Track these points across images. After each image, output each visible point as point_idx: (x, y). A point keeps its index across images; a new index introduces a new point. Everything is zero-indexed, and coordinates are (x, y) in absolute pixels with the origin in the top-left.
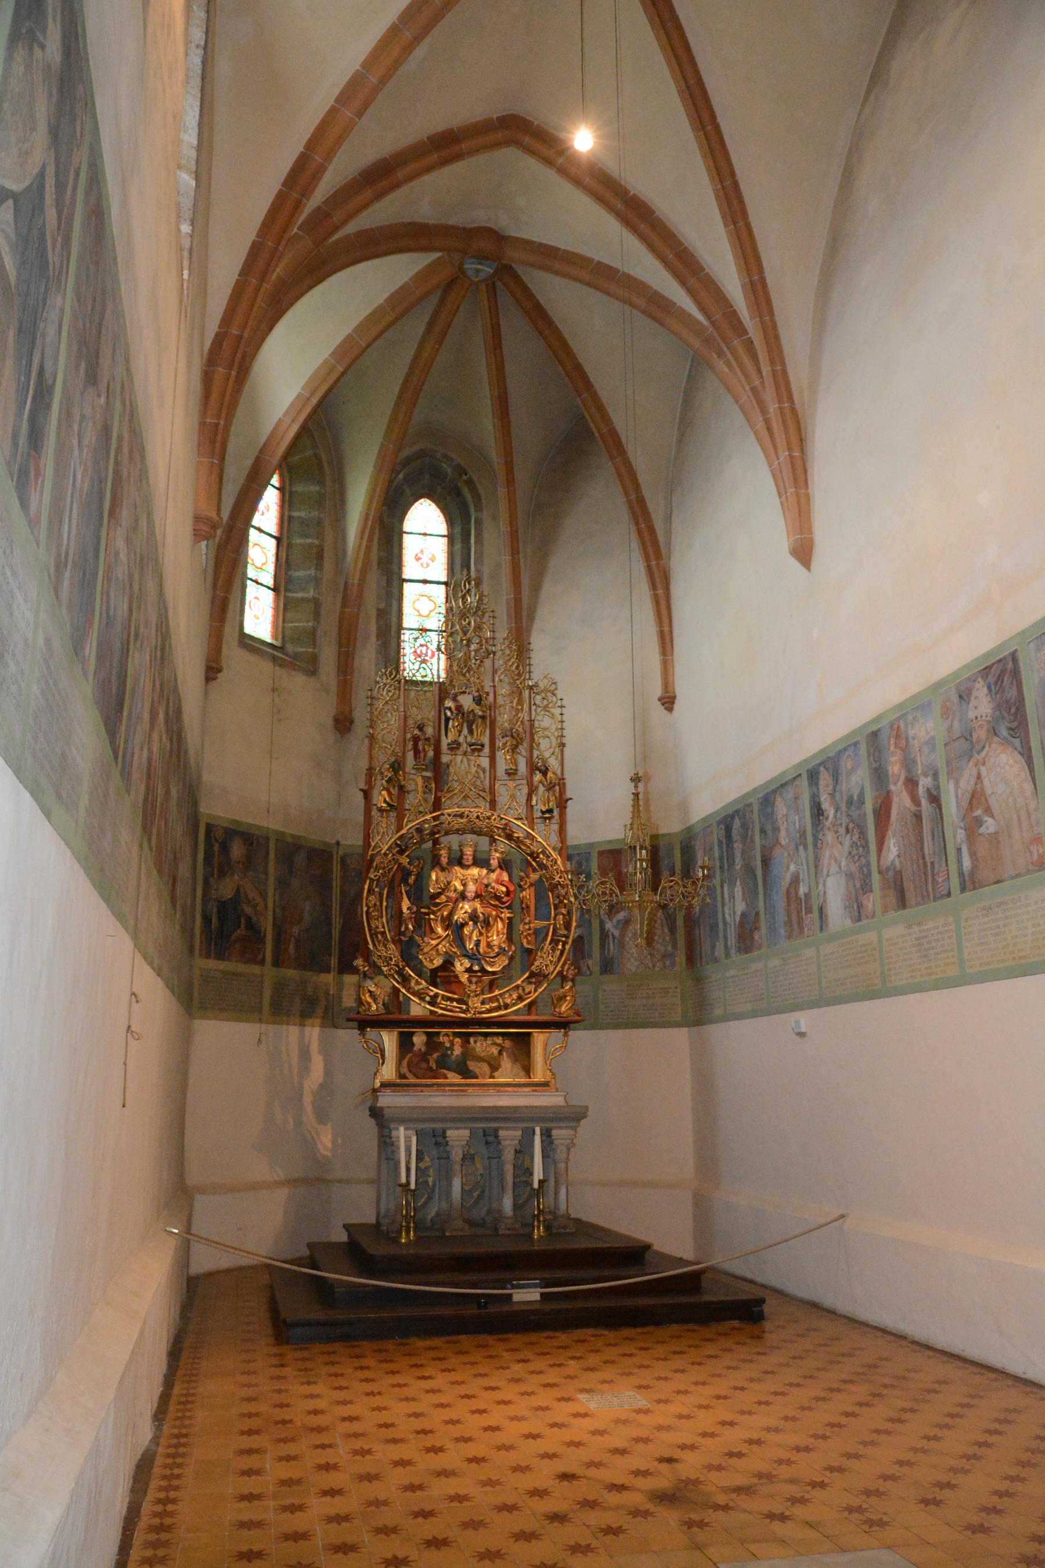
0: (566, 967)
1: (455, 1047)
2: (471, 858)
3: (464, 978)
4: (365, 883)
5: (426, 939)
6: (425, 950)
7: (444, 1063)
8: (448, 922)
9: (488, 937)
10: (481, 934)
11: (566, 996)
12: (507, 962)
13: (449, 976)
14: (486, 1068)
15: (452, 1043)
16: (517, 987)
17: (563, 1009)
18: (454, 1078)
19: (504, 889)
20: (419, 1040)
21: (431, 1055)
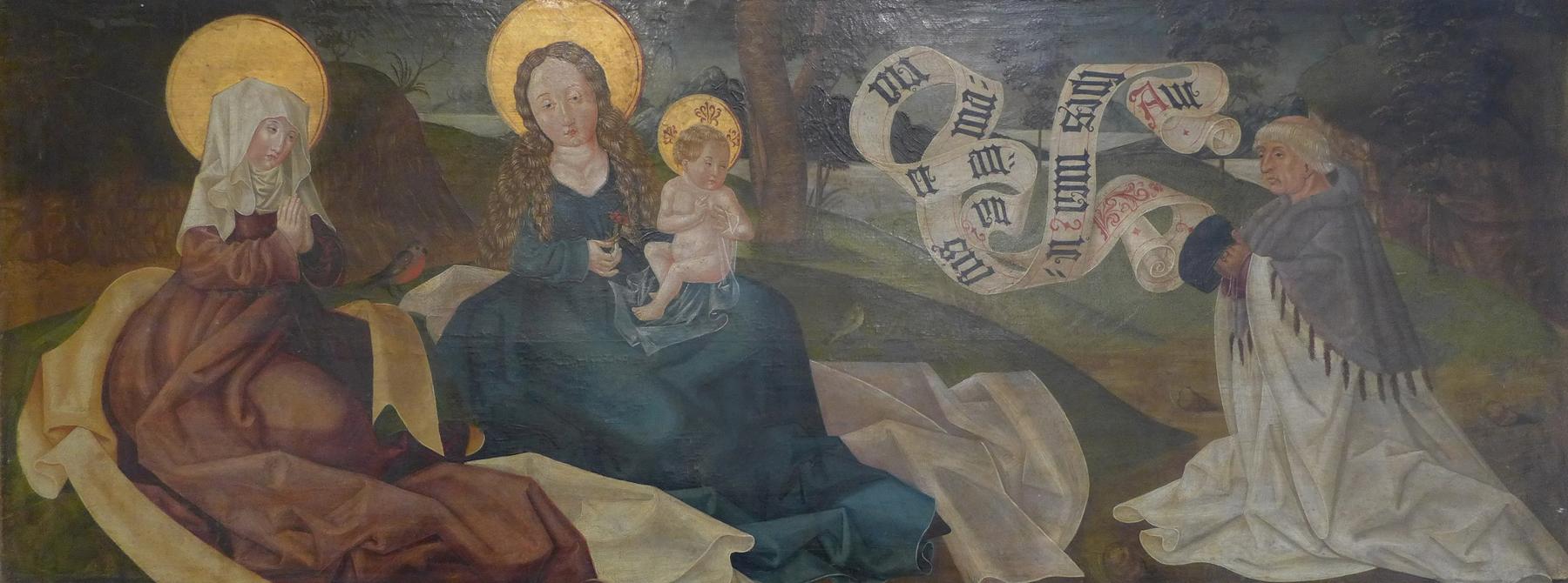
1: (677, 203)
21: (385, 285)
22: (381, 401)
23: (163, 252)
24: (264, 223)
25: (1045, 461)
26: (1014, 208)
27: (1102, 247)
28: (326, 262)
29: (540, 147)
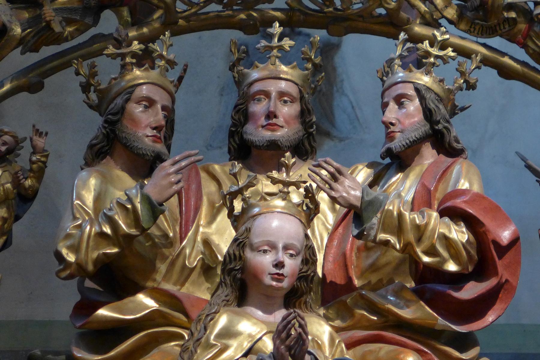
2: (287, 111)
19: (459, 234)
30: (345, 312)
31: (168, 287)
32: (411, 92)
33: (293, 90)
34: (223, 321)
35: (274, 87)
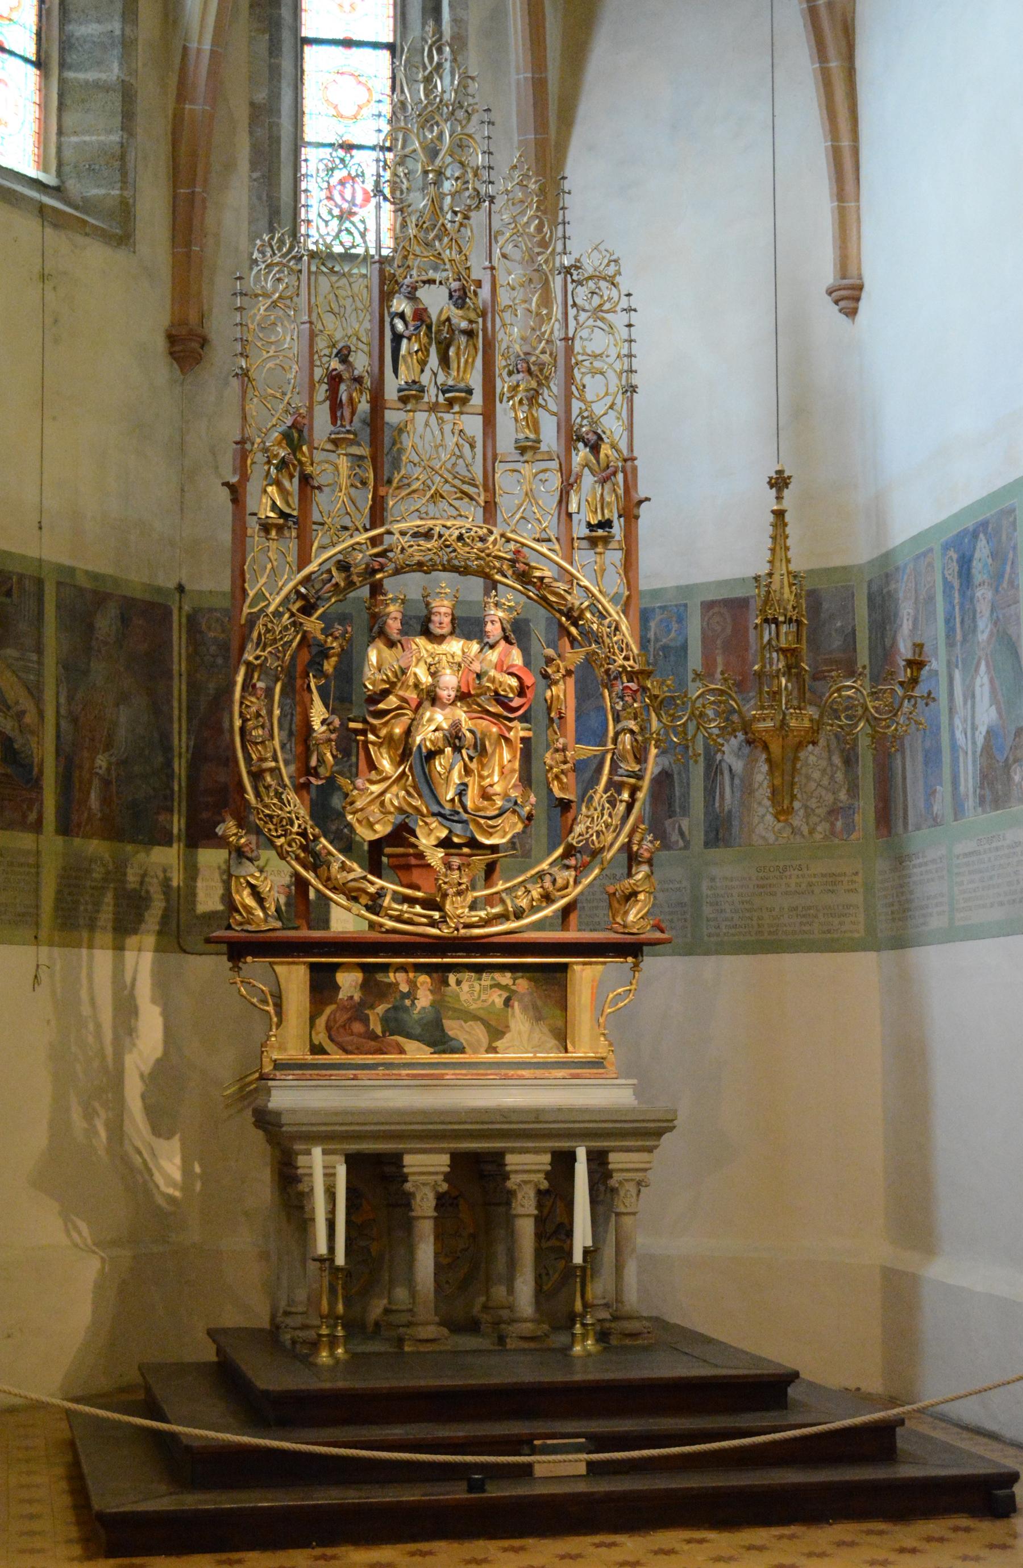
0: (637, 838)
2: (447, 620)
3: (436, 857)
4: (236, 671)
5: (359, 782)
6: (359, 804)
7: (396, 1024)
8: (404, 752)
9: (481, 777)
10: (468, 771)
11: (634, 894)
12: (520, 827)
13: (408, 855)
14: (479, 1032)
15: (413, 984)
16: (540, 876)
17: (631, 917)
18: (417, 1052)
20: (349, 982)
21: (372, 1007)
22: (371, 1027)
23: (336, 1003)
24: (351, 998)
25: (481, 1036)
26: (476, 994)
27: (490, 1000)
28: (362, 1004)
29: (397, 984)
30: (469, 706)
31: (401, 693)
32: (497, 619)
33: (449, 611)
34: (428, 714)
35: (443, 610)
